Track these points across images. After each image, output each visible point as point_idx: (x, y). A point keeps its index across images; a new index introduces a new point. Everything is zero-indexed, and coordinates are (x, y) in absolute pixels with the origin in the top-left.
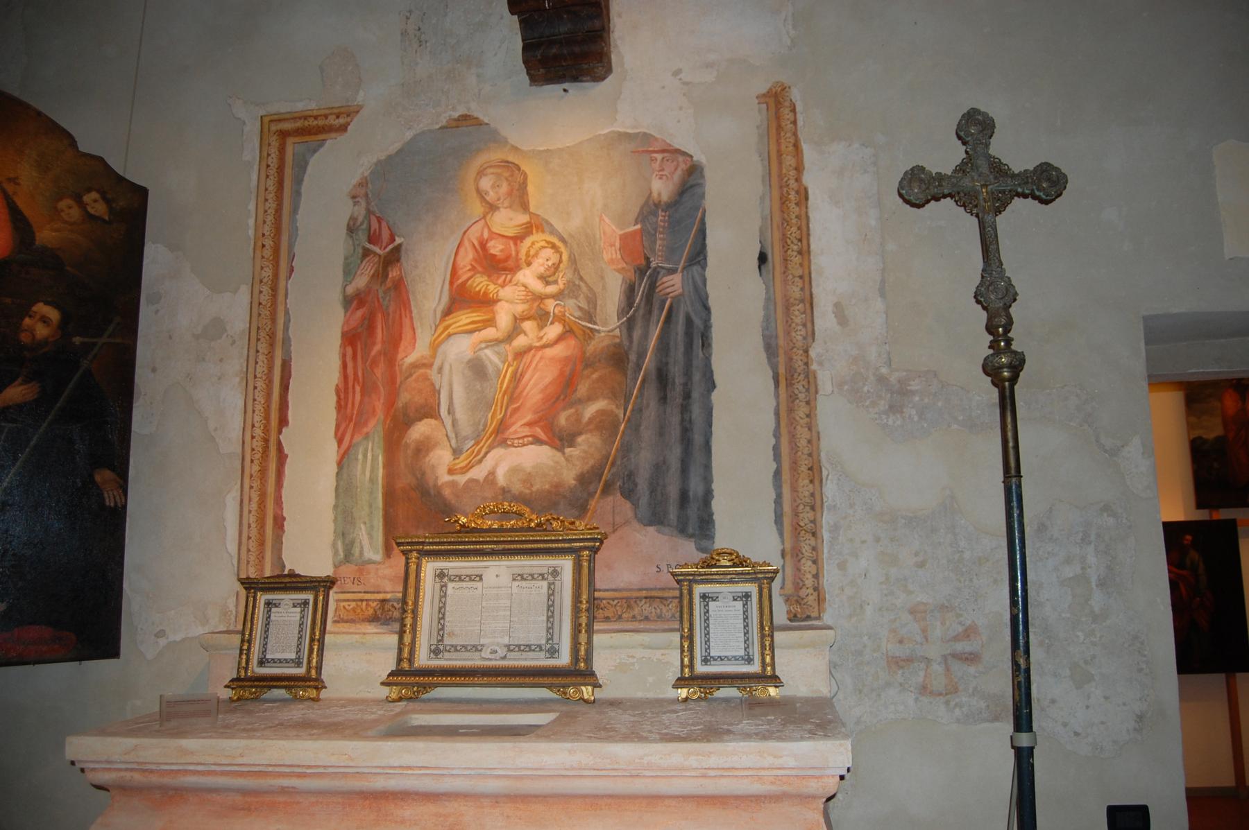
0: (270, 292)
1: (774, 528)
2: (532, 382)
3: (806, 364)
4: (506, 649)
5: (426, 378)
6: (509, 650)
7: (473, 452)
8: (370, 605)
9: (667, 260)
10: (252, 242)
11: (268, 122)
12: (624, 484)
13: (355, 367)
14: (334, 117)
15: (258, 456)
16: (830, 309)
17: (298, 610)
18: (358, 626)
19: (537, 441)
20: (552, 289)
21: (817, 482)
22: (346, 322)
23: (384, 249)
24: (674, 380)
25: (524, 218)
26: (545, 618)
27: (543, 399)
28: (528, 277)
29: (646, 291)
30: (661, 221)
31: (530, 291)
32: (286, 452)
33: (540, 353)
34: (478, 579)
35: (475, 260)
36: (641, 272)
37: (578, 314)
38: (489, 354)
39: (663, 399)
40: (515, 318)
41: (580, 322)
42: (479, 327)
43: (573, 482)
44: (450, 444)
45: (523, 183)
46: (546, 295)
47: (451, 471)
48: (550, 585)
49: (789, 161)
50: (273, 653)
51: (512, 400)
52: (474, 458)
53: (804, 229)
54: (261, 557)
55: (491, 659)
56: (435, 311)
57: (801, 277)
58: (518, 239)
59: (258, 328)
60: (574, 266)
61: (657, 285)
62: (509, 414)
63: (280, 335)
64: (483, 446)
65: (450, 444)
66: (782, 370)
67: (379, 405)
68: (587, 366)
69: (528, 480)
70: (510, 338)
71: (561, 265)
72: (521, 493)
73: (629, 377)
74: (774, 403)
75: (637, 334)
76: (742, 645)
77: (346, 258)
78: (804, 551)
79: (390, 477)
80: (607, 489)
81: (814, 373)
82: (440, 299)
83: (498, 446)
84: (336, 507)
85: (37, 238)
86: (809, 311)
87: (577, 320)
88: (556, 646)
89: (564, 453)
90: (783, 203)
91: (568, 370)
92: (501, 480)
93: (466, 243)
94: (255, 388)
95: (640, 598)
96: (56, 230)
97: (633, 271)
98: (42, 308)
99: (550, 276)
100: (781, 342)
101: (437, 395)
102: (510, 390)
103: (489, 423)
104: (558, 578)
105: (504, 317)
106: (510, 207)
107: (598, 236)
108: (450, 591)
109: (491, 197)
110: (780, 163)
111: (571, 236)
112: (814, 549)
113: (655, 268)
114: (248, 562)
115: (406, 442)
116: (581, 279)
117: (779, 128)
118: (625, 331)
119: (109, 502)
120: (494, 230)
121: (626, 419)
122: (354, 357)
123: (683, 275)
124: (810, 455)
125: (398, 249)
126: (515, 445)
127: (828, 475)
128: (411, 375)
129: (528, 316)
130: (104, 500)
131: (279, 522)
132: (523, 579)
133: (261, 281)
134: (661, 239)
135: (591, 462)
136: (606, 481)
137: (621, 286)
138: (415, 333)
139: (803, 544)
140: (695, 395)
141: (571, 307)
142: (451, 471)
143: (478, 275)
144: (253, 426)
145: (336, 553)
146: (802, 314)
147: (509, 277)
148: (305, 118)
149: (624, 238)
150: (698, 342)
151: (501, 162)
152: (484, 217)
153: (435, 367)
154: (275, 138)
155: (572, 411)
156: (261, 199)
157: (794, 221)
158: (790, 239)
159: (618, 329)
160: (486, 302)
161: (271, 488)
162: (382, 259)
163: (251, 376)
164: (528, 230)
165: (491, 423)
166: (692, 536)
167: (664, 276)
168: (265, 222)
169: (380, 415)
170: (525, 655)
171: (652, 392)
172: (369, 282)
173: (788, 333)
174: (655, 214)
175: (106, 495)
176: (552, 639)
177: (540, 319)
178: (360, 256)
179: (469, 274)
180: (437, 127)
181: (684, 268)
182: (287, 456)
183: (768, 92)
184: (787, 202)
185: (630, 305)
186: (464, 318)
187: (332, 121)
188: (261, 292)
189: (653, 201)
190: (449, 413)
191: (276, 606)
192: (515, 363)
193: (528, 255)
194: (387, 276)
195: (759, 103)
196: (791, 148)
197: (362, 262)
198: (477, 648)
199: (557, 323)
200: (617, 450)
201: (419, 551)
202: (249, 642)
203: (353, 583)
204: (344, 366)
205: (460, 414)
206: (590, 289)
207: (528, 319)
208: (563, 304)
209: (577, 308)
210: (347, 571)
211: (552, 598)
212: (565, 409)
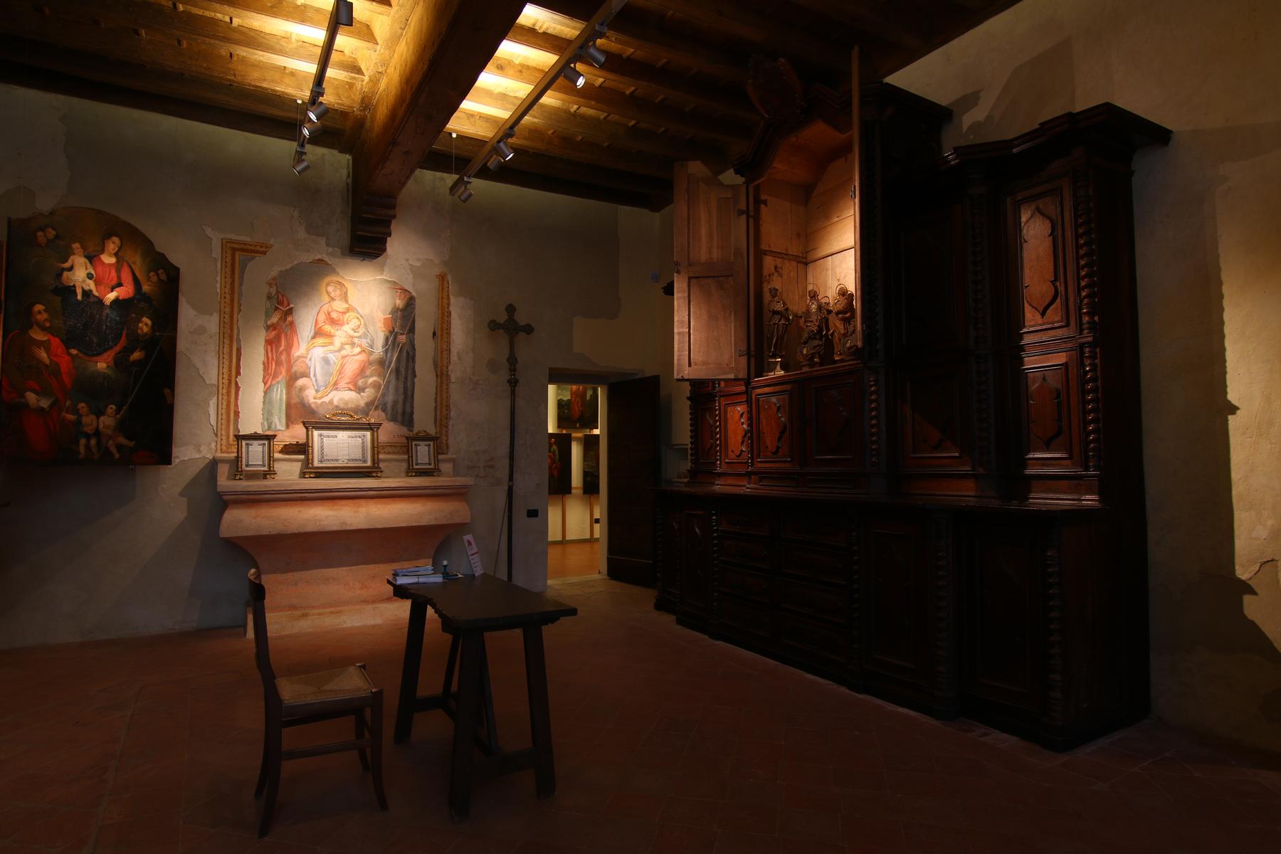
5: (305, 362)
9: (401, 330)
13: (272, 355)
19: (350, 390)
25: (346, 306)
33: (352, 358)
36: (391, 332)
38: (332, 357)
39: (397, 379)
49: (445, 301)
51: (340, 374)
58: (344, 313)
59: (224, 333)
63: (235, 336)
66: (439, 373)
67: (284, 371)
69: (346, 403)
70: (339, 351)
74: (435, 384)
75: (389, 355)
77: (267, 309)
80: (376, 408)
91: (362, 365)
92: (336, 402)
93: (321, 311)
98: (145, 319)
105: (338, 342)
109: (332, 295)
114: (221, 429)
117: (443, 289)
119: (169, 402)
122: (272, 350)
131: (237, 413)
135: (371, 399)
140: (409, 378)
141: (364, 342)
142: (315, 398)
149: (385, 319)
152: (330, 302)
153: (309, 357)
155: (363, 380)
156: (223, 276)
161: (233, 399)
164: (348, 310)
168: (225, 287)
171: (393, 376)
174: (397, 312)
186: (320, 341)
187: (258, 248)
193: (347, 320)
194: (286, 319)
198: (337, 460)
205: (319, 377)
212: (361, 379)
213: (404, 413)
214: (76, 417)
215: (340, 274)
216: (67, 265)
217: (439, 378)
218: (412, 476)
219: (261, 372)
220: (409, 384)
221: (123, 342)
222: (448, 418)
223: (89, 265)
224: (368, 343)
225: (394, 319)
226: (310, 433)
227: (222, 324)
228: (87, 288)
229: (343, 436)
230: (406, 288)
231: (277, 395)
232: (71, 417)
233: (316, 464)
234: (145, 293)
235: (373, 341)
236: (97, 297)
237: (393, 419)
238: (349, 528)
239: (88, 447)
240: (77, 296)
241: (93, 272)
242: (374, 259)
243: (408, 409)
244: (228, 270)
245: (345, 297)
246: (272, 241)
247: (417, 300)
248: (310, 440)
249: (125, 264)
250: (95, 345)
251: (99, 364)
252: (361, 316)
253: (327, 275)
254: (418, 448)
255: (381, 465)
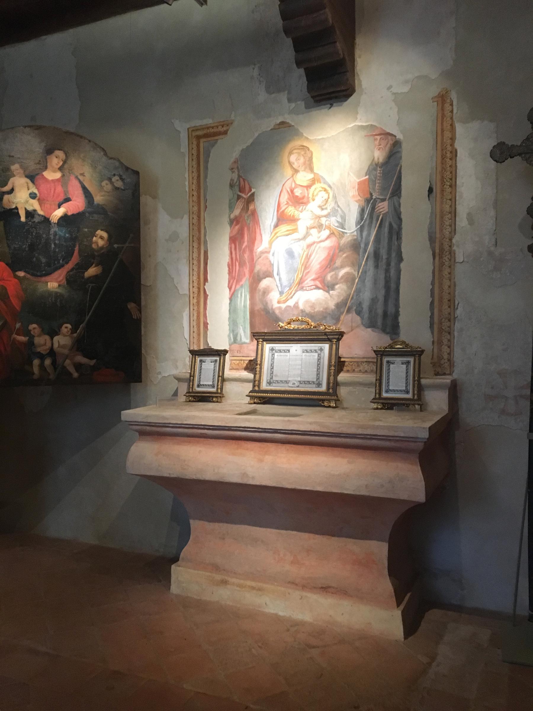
0: (197, 218)
1: (430, 330)
2: (315, 260)
3: (450, 246)
4: (299, 383)
5: (267, 258)
6: (301, 383)
7: (289, 293)
8: (245, 362)
10: (188, 194)
11: (191, 131)
12: (357, 308)
13: (236, 254)
14: (221, 127)
15: (196, 295)
16: (465, 216)
17: (213, 364)
18: (240, 371)
19: (317, 288)
20: (325, 212)
21: (452, 307)
22: (231, 232)
23: (247, 194)
24: (382, 256)
25: (311, 176)
26: (316, 370)
27: (320, 267)
28: (313, 207)
29: (370, 211)
30: (379, 173)
31: (314, 214)
32: (208, 293)
33: (318, 245)
34: (288, 351)
35: (288, 199)
36: (368, 201)
37: (337, 224)
39: (377, 267)
40: (307, 228)
41: (338, 228)
42: (290, 233)
43: (334, 307)
44: (278, 290)
45: (311, 157)
46: (322, 215)
47: (279, 302)
48: (319, 355)
49: (447, 134)
50: (203, 382)
51: (306, 268)
52: (289, 296)
53: (454, 173)
54: (199, 340)
55: (292, 387)
56: (271, 225)
57: (450, 200)
58: (308, 187)
59: (193, 236)
60: (335, 200)
61: (376, 207)
62: (304, 275)
64: (292, 291)
65: (278, 290)
66: (437, 251)
67: (247, 271)
68: (340, 251)
69: (313, 306)
70: (304, 238)
71: (329, 200)
72: (310, 312)
73: (360, 256)
75: (365, 234)
76: (404, 385)
77: (230, 200)
78: (444, 341)
79: (252, 304)
80: (349, 311)
81: (454, 251)
82: (273, 220)
83: (300, 290)
84: (229, 318)
85: (95, 200)
86: (453, 219)
87: (336, 228)
88: (321, 382)
89: (329, 293)
90: (443, 159)
91: (332, 253)
92: (301, 306)
93: (284, 191)
94: (193, 264)
95: (363, 362)
96: (102, 196)
97: (364, 201)
98: (100, 232)
99: (323, 206)
100: (438, 235)
101: (272, 266)
102: (305, 263)
103: (295, 280)
104: (323, 352)
106: (305, 170)
107: (347, 184)
108: (276, 357)
110: (442, 136)
111: (334, 184)
112: (449, 340)
113: (375, 199)
114: (194, 343)
115: (259, 289)
116: (338, 206)
117: (443, 116)
118: (359, 232)
119: (135, 317)
120: (298, 183)
121: (359, 275)
123: (388, 202)
124: (449, 294)
125: (253, 194)
126: (307, 289)
127: (458, 304)
128: (260, 257)
129: (313, 226)
130: (132, 316)
131: (206, 325)
132: (307, 352)
133: (193, 213)
134: (378, 183)
135: (342, 298)
136: (349, 307)
137: (358, 209)
138: (262, 237)
139: (443, 338)
140: (393, 264)
141: (333, 221)
142: (279, 302)
143: (290, 207)
144: (193, 282)
145: (230, 339)
146: (450, 220)
147: (304, 207)
148: (208, 128)
149: (360, 184)
150: (395, 237)
151: (300, 146)
152: (293, 176)
154: (195, 139)
155: (333, 273)
156: (191, 171)
157: (448, 169)
158: (446, 179)
159: (356, 232)
160: (293, 220)
161: (202, 310)
162: (246, 200)
163: (191, 259)
164: (313, 182)
165: (297, 279)
166: (387, 333)
167: (380, 202)
168: (193, 183)
169: (247, 275)
170: (307, 385)
171: (371, 263)
172: (241, 212)
173: (441, 230)
175: (133, 314)
176: (319, 379)
177: (319, 228)
178: (236, 199)
179: (286, 206)
180: (270, 129)
181: (389, 198)
182: (208, 295)
183: (438, 95)
184: (445, 158)
185: (362, 219)
186: (284, 228)
187: (220, 129)
188: (193, 218)
189: (375, 162)
190: (278, 275)
191: (204, 362)
192: (307, 251)
193: (313, 196)
194: (248, 209)
195: (433, 102)
196: (449, 127)
197: (237, 202)
198: (287, 382)
199: (326, 230)
200: (354, 292)
201: (262, 339)
202: (193, 377)
203: (238, 352)
204: (231, 253)
206: (343, 211)
207: (314, 228)
208: (329, 219)
209: (336, 222)
210: (235, 347)
211: (320, 361)
212: (330, 272)
213: (385, 314)
214: (27, 338)
215: (305, 135)
216: (6, 188)
217: (437, 258)
218: (377, 409)
219: (227, 276)
220: (393, 272)
221: (75, 259)
222: (451, 318)
223: (31, 184)
224: (338, 222)
225: (371, 181)
226: (260, 345)
227: (191, 225)
228: (30, 208)
229: (296, 349)
230: (388, 131)
231: (241, 301)
232: (22, 339)
233: (264, 386)
234: (98, 205)
235: (343, 218)
236: (42, 216)
237: (371, 324)
238: (251, 482)
239: (42, 366)
240: (20, 217)
241: (36, 191)
242: (346, 101)
243: (391, 309)
244: (194, 163)
245: (309, 166)
246: (233, 117)
247: (404, 146)
248: (259, 356)
249: (72, 178)
250: (43, 265)
251: (49, 283)
252: (330, 186)
253: (289, 141)
254: (391, 366)
255: (343, 391)
